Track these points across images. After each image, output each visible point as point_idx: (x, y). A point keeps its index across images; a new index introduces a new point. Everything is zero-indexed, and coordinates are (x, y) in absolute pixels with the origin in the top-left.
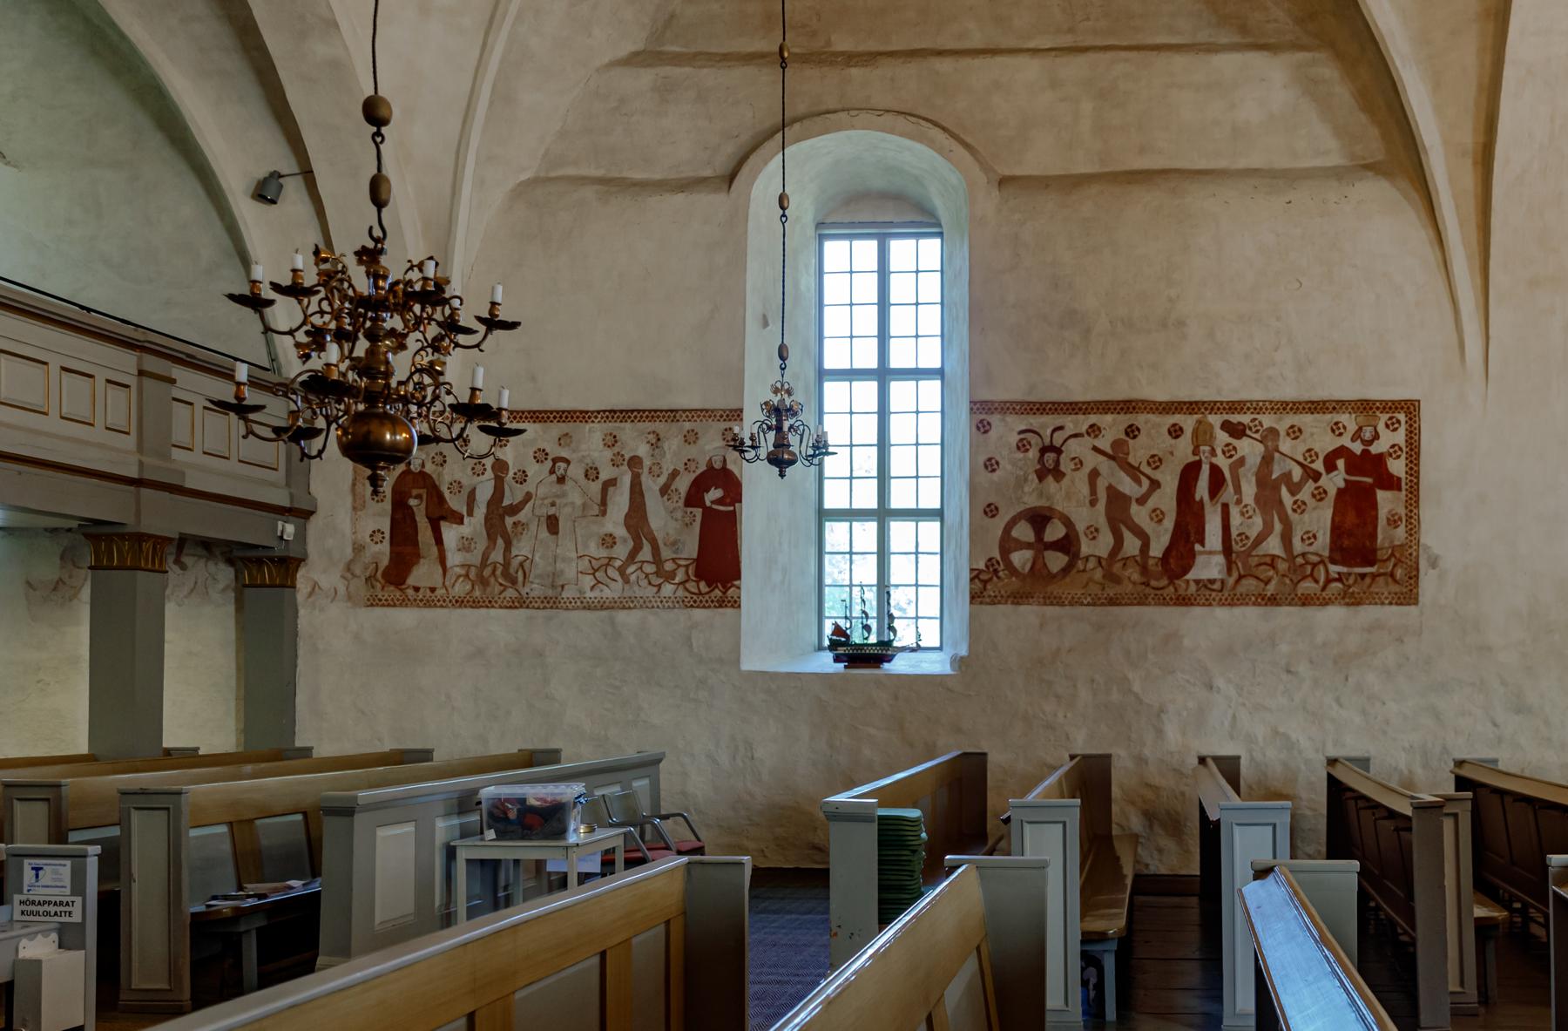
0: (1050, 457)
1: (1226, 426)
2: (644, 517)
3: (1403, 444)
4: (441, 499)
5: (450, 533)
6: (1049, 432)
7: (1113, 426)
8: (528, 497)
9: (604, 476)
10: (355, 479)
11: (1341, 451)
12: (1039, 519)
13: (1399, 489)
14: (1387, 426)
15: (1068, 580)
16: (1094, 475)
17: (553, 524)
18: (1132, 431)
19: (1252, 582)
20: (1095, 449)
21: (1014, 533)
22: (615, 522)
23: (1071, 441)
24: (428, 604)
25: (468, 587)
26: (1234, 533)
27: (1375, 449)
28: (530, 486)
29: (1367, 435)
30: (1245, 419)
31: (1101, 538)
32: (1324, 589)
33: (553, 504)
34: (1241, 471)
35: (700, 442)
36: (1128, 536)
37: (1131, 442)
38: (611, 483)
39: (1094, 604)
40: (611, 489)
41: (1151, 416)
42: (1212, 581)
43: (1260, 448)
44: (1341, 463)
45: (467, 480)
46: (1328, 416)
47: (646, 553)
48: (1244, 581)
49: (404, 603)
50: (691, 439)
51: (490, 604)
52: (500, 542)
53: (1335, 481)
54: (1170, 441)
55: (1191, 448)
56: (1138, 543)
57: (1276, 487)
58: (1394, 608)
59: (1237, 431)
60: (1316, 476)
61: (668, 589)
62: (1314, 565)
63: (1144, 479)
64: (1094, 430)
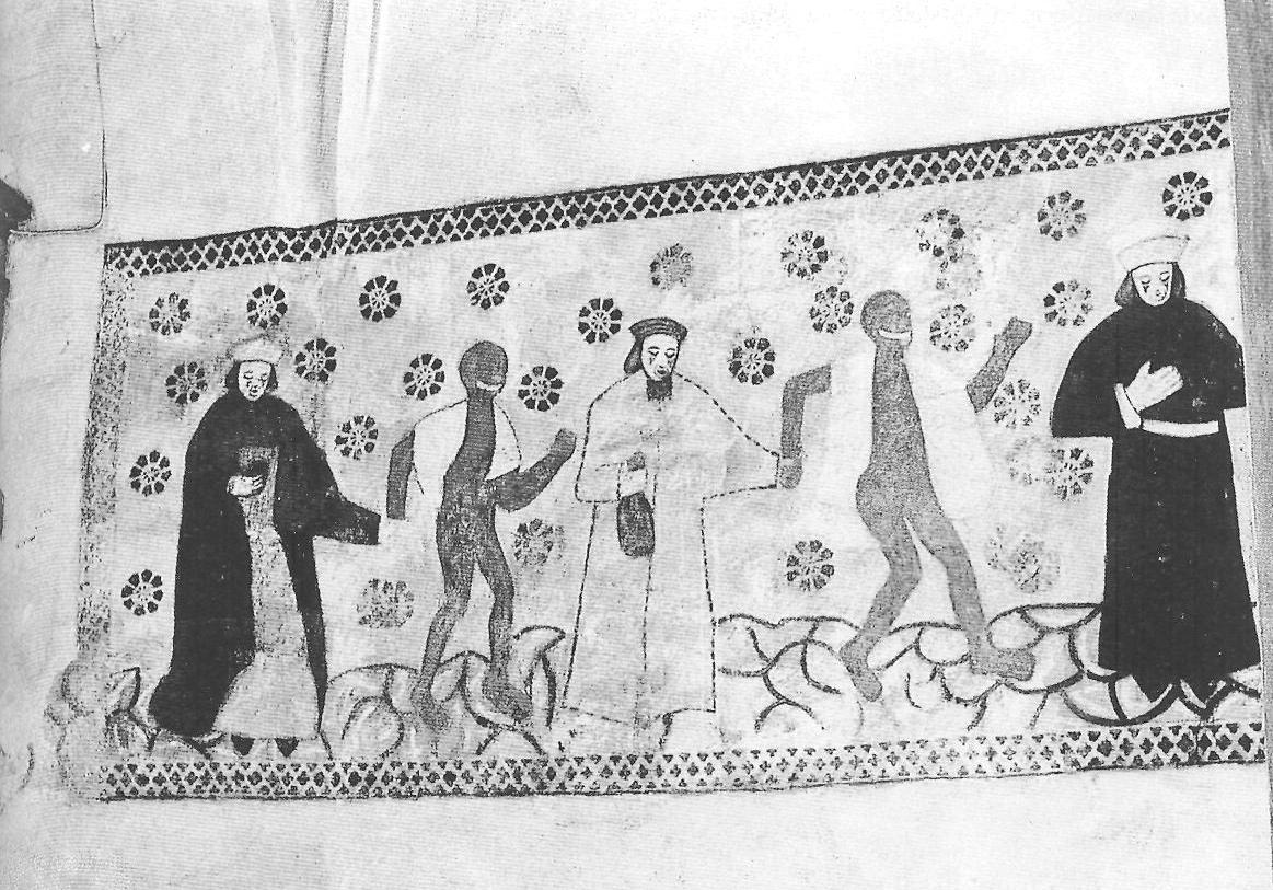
2: (922, 480)
4: (319, 471)
5: (341, 569)
8: (562, 451)
9: (786, 368)
10: (92, 434)
17: (636, 522)
22: (827, 505)
24: (274, 790)
25: (389, 734)
28: (568, 415)
33: (637, 464)
35: (1093, 226)
38: (815, 381)
40: (812, 402)
45: (391, 415)
47: (930, 598)
49: (208, 787)
50: (1061, 219)
51: (449, 784)
52: (481, 588)
61: (1010, 712)
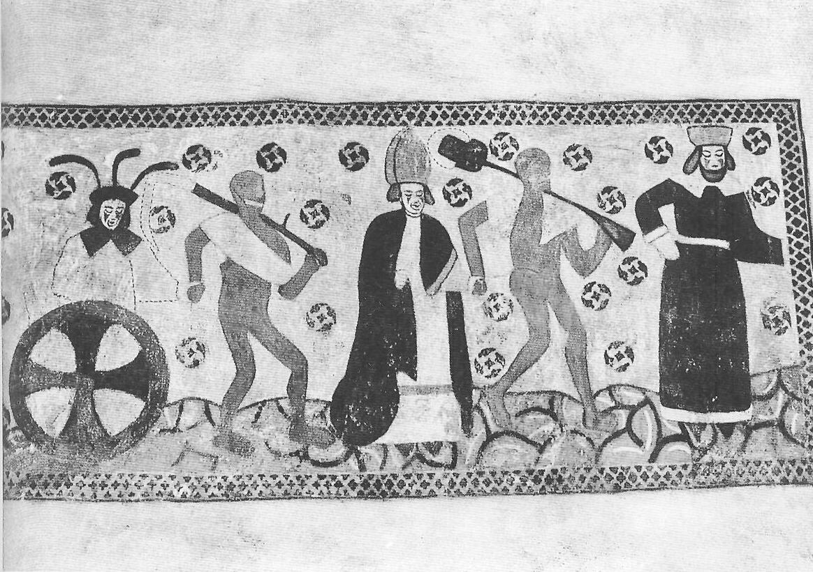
0: (111, 208)
1: (452, 148)
3: (778, 180)
6: (109, 162)
7: (234, 148)
11: (667, 192)
12: (84, 326)
13: (780, 261)
14: (747, 145)
15: (143, 447)
16: (198, 239)
18: (270, 157)
19: (520, 447)
20: (200, 191)
21: (37, 356)
23: (152, 177)
26: (473, 351)
27: (728, 187)
29: (713, 161)
30: (484, 133)
31: (209, 363)
32: (653, 458)
34: (482, 231)
36: (263, 358)
37: (268, 177)
39: (197, 499)
41: (305, 129)
42: (435, 447)
43: (514, 189)
44: (667, 212)
46: (636, 129)
48: (497, 445)
53: (661, 246)
54: (341, 176)
55: (386, 187)
56: (285, 373)
57: (550, 262)
58: (790, 489)
59: (468, 156)
60: (625, 239)
62: (633, 410)
63: (293, 247)
64: (197, 156)
